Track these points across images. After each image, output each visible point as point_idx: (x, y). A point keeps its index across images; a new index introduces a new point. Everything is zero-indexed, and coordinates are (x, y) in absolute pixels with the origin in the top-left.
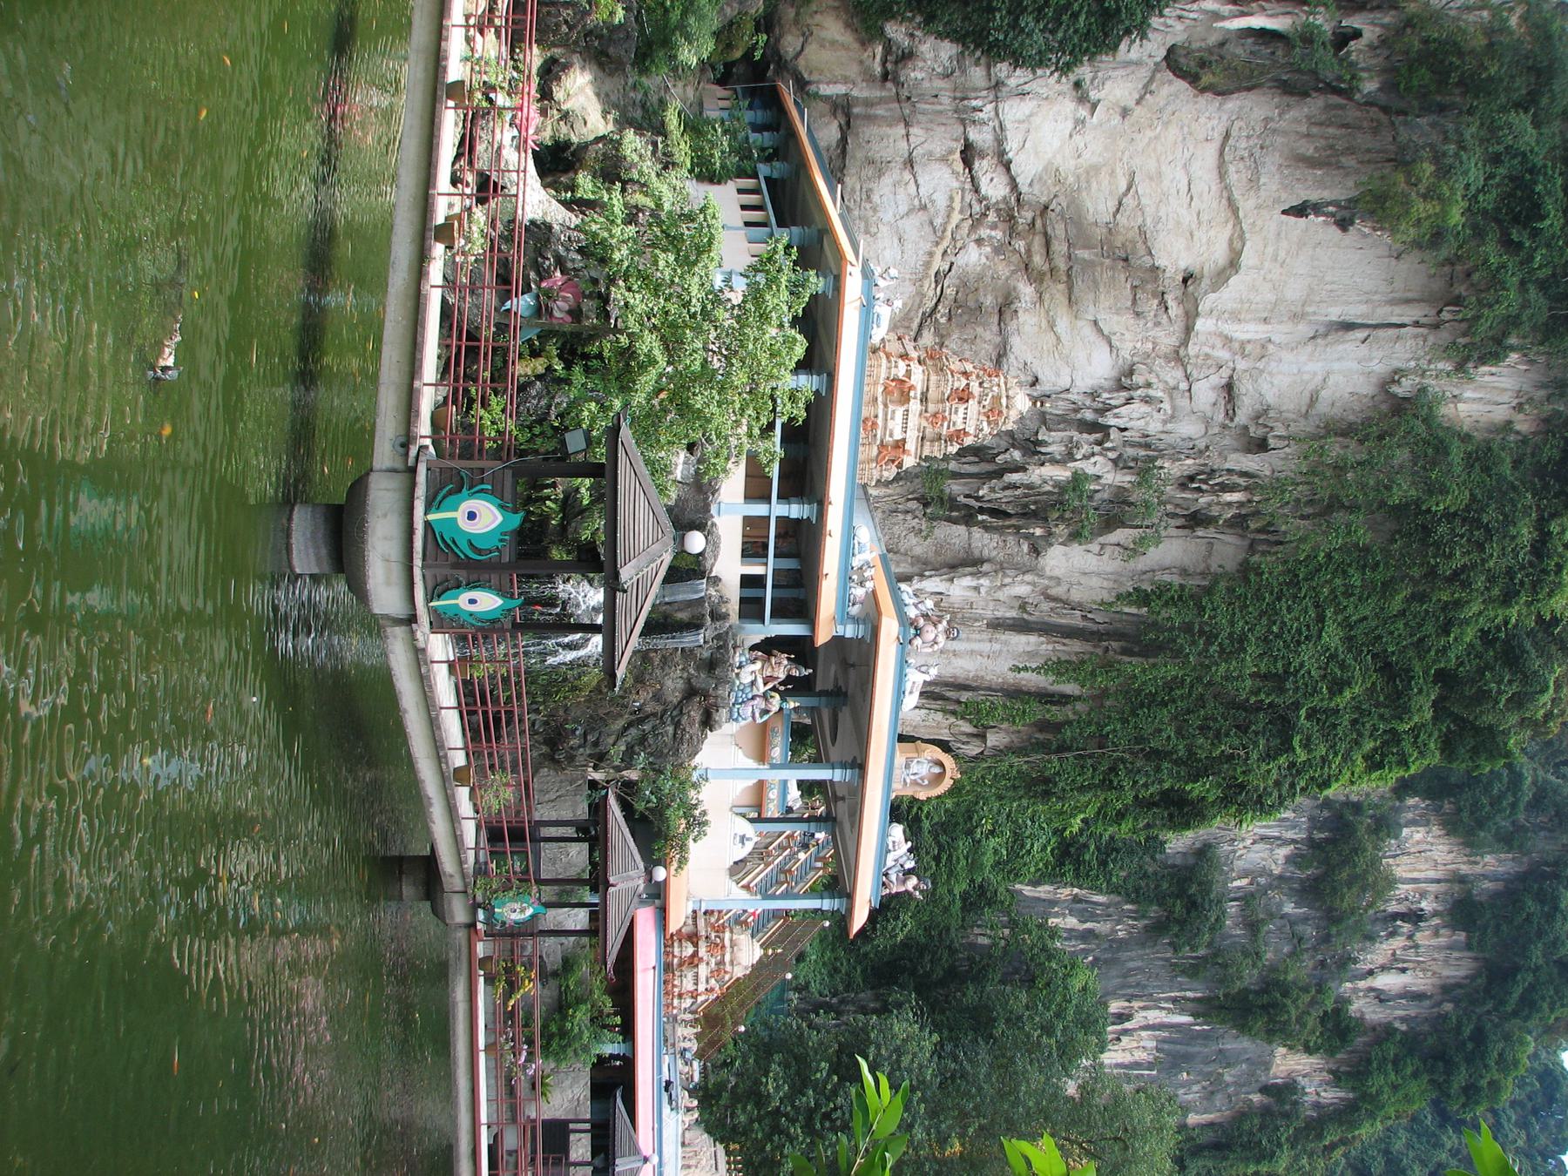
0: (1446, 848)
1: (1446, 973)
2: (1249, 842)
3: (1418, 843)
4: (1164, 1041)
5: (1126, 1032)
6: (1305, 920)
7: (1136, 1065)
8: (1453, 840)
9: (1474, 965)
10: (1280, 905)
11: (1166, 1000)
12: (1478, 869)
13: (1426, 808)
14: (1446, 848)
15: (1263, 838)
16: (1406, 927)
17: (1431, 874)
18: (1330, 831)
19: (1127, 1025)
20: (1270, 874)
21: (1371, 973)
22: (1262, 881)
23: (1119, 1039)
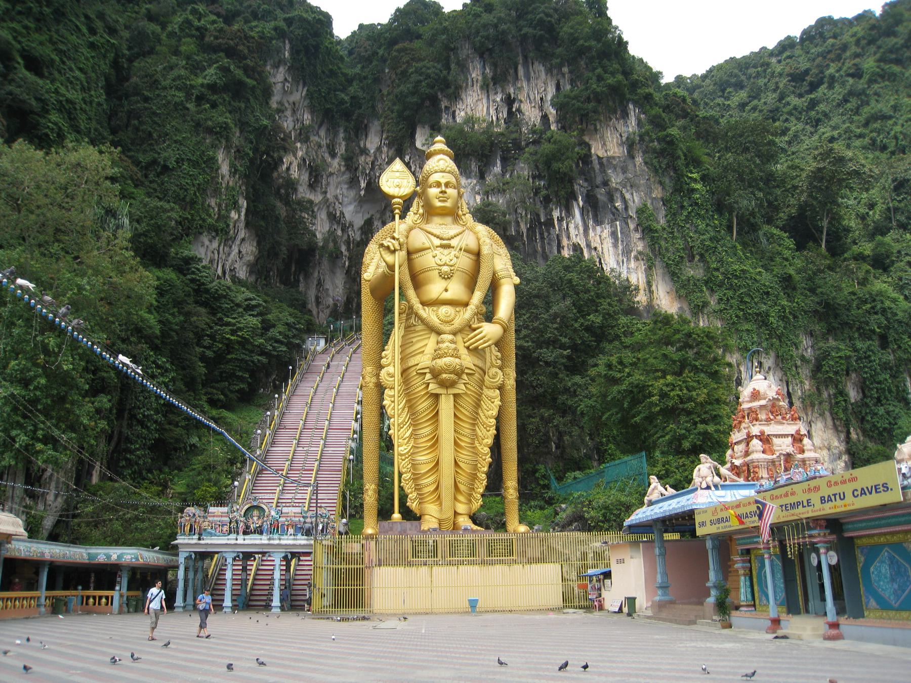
0: (469, 98)
4: (594, 222)
5: (588, 246)
6: (504, 160)
7: (614, 234)
8: (463, 96)
9: (536, 64)
10: (495, 175)
11: (560, 226)
12: (480, 78)
13: (448, 114)
16: (516, 105)
17: (485, 101)
19: (583, 245)
20: (476, 185)
21: (545, 118)
22: (477, 188)
23: (595, 249)
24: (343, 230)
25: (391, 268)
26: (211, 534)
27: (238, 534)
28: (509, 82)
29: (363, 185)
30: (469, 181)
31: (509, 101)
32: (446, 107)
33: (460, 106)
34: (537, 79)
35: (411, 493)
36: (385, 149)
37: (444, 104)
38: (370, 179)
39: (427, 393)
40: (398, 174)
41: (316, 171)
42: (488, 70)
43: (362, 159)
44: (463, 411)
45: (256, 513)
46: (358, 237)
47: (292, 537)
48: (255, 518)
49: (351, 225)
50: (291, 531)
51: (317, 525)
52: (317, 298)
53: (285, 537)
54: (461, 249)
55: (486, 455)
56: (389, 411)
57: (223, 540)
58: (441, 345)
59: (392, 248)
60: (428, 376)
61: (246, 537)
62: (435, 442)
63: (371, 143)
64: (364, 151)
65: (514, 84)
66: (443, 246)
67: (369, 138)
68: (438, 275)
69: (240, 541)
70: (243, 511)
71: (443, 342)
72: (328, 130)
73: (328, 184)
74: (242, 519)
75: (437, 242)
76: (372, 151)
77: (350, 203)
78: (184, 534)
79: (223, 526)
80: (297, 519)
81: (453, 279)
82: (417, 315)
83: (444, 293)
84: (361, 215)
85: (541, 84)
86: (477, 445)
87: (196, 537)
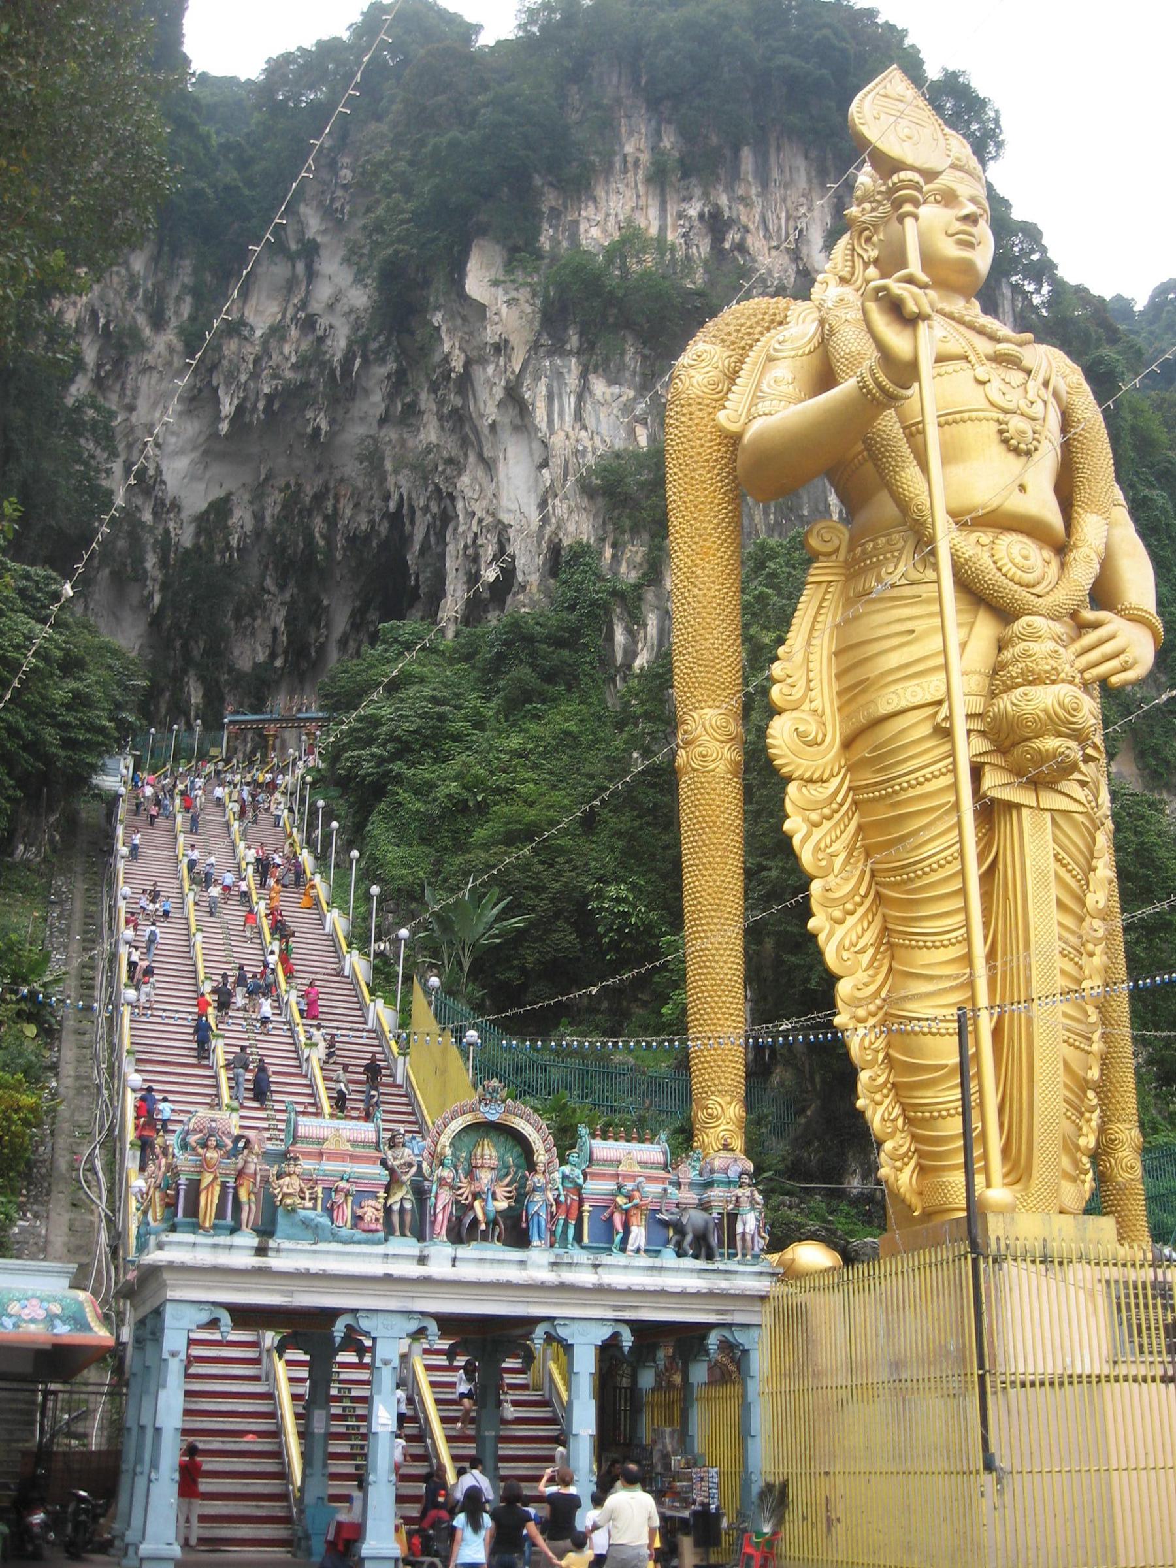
0: (614, 198)
1: (802, 183)
2: (583, 434)
3: (604, 231)
8: (600, 192)
12: (645, 158)
13: (556, 228)
14: (614, 198)
15: (579, 416)
16: (733, 236)
17: (653, 213)
18: (566, 329)
22: (641, 407)
24: (155, 514)
26: (314, 1232)
27: (421, 1237)
28: (718, 179)
29: (227, 407)
30: (616, 389)
31: (716, 224)
32: (552, 209)
33: (589, 211)
34: (787, 186)
35: (892, 1135)
36: (294, 332)
37: (550, 199)
38: (245, 399)
41: (121, 346)
42: (667, 143)
43: (231, 347)
45: (489, 1152)
46: (186, 537)
47: (644, 1260)
48: (485, 1176)
49: (176, 506)
50: (638, 1235)
51: (732, 1217)
53: (617, 1258)
54: (1046, 384)
56: (806, 858)
57: (365, 1260)
58: (1034, 647)
61: (463, 1251)
63: (258, 312)
64: (236, 329)
65: (730, 188)
66: (999, 359)
67: (253, 301)
68: (995, 438)
69: (439, 1268)
70: (445, 1140)
71: (1035, 637)
72: (155, 259)
73: (136, 390)
74: (446, 1173)
76: (258, 333)
77: (181, 452)
78: (195, 1227)
79: (360, 1197)
80: (657, 1189)
81: (1036, 456)
84: (201, 487)
85: (794, 195)
87: (247, 1239)
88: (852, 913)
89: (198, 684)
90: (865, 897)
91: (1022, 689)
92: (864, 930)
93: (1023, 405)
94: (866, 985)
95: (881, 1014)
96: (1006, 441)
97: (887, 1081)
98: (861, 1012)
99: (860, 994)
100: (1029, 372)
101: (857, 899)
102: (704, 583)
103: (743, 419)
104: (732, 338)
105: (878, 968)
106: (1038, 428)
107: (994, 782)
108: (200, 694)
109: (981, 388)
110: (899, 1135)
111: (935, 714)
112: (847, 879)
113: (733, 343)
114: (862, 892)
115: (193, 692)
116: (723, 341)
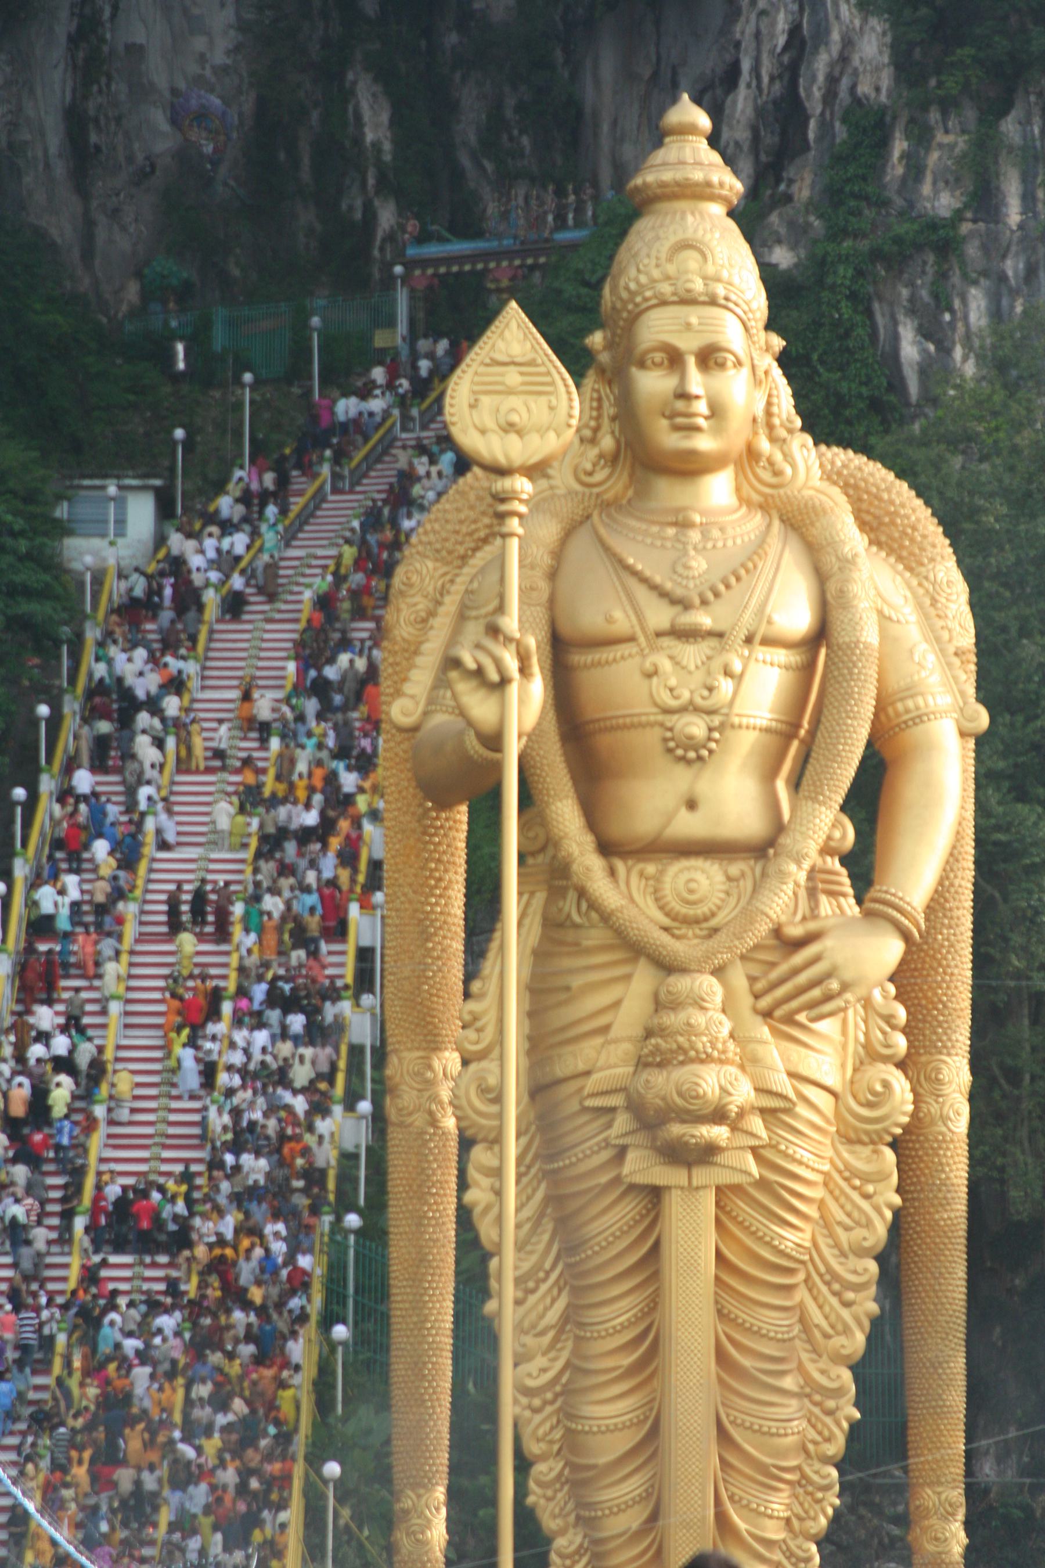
25: (494, 741)
35: (563, 1532)
39: (617, 1180)
40: (513, 377)
44: (749, 1242)
52: (76, 121)
54: (749, 640)
55: (838, 1393)
59: (494, 676)
60: (622, 1122)
62: (649, 1350)
68: (659, 748)
71: (675, 1005)
75: (660, 615)
82: (582, 893)
83: (683, 811)
86: (805, 1356)
88: (533, 1291)
89: (378, 88)
90: (548, 1274)
91: (645, 1076)
92: (546, 1309)
93: (698, 701)
94: (544, 1370)
95: (558, 1404)
96: (670, 751)
97: (561, 1474)
98: (537, 1402)
99: (531, 1383)
100: (720, 635)
101: (541, 1275)
102: (405, 895)
103: (420, 709)
104: (449, 545)
105: (562, 1349)
106: (716, 720)
107: (641, 1167)
108: (385, 117)
109: (646, 682)
110: (571, 1531)
111: (582, 1089)
112: (531, 1252)
113: (450, 552)
114: (547, 1265)
115: (367, 115)
116: (437, 551)
